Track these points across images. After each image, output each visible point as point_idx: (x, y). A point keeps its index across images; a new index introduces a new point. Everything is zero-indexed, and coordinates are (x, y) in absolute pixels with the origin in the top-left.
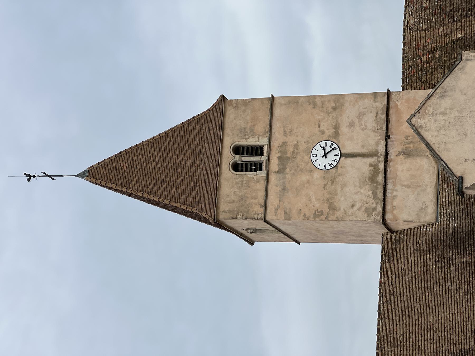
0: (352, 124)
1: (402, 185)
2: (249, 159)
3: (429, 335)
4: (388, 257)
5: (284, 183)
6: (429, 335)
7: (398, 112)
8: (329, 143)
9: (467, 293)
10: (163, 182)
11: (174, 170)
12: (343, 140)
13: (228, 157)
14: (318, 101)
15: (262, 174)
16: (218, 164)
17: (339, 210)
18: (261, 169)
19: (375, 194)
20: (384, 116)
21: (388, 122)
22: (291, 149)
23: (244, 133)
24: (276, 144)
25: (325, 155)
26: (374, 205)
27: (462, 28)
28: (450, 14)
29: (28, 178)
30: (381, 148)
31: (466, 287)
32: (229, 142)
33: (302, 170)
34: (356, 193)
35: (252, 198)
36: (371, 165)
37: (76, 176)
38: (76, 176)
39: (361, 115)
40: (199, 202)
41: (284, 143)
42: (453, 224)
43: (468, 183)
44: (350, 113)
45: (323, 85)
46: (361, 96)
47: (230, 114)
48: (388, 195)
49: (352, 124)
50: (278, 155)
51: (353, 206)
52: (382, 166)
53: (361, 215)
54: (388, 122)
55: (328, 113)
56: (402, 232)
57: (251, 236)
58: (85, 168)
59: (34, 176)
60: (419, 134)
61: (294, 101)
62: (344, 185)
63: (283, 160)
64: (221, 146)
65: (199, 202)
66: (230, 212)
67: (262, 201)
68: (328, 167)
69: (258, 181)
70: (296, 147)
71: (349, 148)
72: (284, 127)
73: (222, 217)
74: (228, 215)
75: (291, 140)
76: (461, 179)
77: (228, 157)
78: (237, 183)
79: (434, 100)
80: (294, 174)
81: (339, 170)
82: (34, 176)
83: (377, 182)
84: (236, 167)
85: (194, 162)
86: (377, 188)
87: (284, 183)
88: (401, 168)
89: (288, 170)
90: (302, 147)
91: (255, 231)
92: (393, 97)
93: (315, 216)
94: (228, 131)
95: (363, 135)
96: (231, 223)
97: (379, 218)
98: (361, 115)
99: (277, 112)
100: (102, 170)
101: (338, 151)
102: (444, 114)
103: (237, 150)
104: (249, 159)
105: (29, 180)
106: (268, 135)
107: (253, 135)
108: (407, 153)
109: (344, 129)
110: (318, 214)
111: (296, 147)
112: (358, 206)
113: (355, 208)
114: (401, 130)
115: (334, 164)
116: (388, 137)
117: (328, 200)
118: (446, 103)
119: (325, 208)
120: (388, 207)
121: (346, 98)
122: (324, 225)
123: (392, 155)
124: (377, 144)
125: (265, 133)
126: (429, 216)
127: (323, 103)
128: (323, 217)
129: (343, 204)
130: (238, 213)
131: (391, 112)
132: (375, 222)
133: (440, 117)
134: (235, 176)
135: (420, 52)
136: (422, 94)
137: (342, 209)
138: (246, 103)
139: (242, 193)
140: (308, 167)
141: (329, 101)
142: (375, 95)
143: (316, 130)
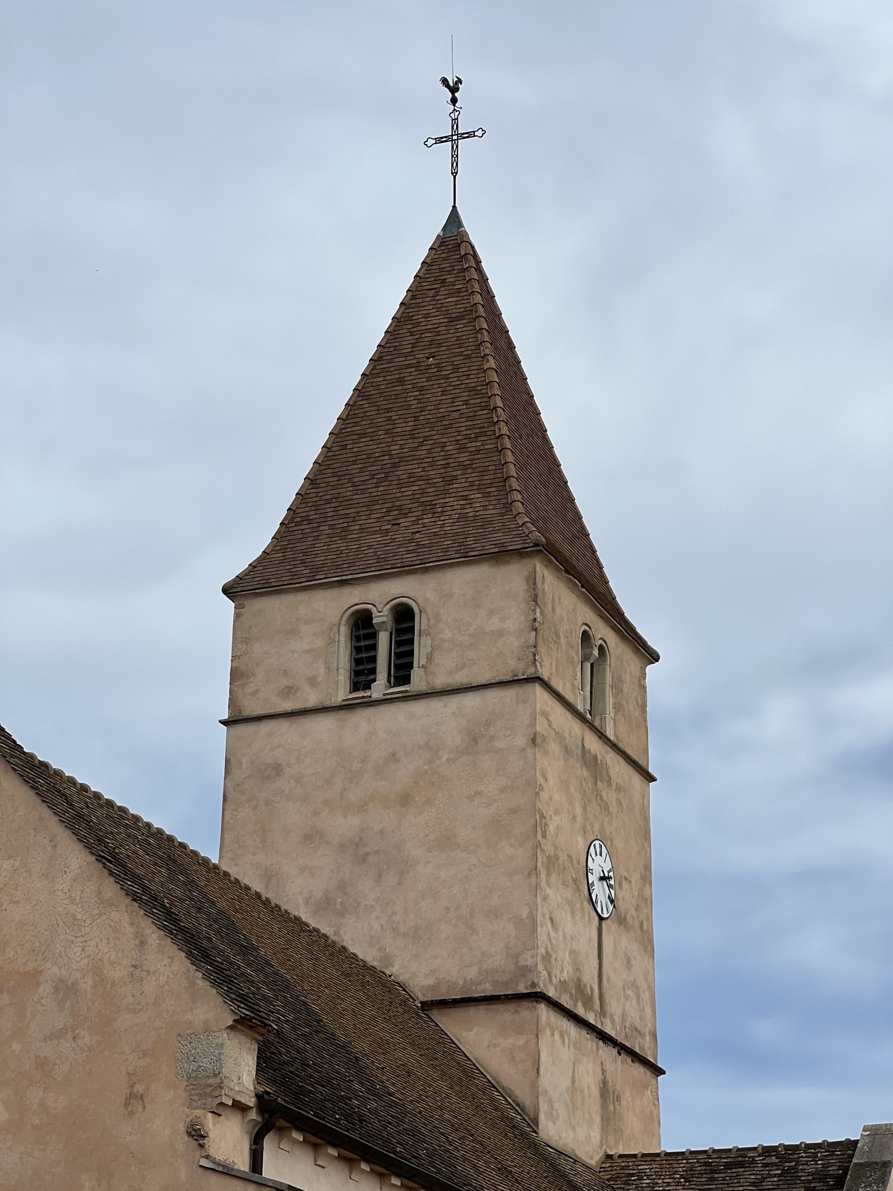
22: (604, 794)
29: (451, 84)
30: (608, 1029)
34: (564, 934)
37: (454, 207)
38: (454, 207)
48: (566, 1025)
49: (629, 965)
59: (454, 101)
70: (607, 809)
81: (588, 907)
82: (454, 101)
105: (445, 81)
116: (622, 1049)
119: (549, 849)
123: (607, 1052)
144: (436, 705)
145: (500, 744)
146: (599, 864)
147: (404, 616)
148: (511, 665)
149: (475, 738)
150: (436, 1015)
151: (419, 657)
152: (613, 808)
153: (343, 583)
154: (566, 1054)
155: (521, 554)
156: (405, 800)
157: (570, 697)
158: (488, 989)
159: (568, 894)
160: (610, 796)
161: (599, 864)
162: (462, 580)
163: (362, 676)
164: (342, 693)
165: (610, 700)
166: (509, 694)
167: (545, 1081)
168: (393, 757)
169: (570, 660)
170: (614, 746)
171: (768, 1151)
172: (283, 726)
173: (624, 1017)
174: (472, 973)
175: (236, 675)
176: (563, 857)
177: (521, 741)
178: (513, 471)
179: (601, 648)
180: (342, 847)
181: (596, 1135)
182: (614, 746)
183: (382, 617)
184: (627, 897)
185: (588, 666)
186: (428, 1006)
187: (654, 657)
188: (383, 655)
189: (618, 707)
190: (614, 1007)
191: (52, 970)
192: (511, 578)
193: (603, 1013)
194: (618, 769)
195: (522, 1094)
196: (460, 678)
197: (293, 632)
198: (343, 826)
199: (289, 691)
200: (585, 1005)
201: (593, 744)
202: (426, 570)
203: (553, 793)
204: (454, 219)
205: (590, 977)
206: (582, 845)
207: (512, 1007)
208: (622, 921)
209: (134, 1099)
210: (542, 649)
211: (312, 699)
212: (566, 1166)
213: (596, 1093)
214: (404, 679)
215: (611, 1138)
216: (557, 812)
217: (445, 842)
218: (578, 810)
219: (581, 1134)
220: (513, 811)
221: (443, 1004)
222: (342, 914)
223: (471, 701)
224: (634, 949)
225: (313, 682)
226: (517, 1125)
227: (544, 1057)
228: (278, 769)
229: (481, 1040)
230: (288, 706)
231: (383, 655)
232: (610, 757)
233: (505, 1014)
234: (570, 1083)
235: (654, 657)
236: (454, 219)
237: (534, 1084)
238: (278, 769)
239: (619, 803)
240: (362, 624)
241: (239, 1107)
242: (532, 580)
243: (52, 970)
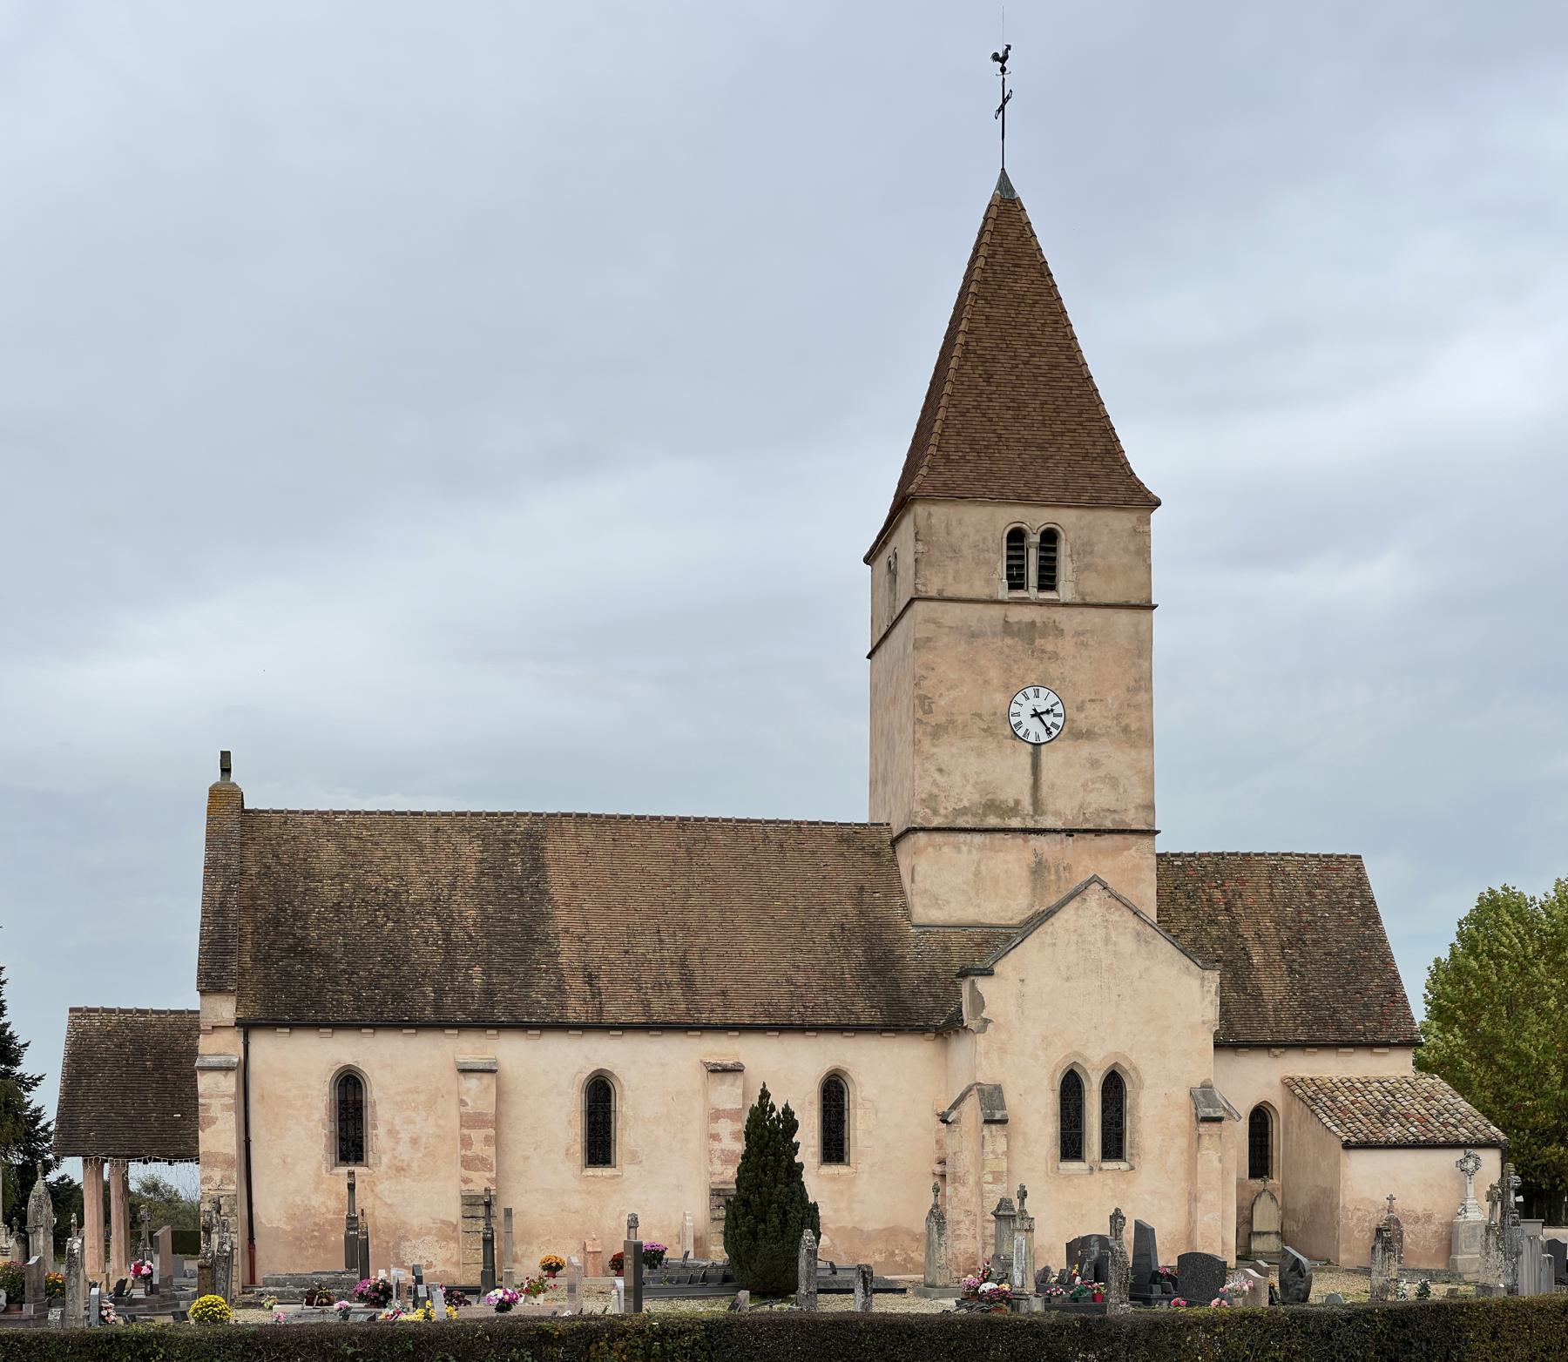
0: (1095, 764)
1: (979, 863)
2: (1032, 562)
3: (713, 914)
4: (848, 836)
5: (984, 634)
6: (713, 914)
7: (1117, 851)
8: (1059, 721)
9: (789, 981)
10: (988, 378)
11: (1013, 401)
13: (1035, 519)
14: (1141, 697)
15: (1003, 592)
16: (1022, 500)
17: (934, 745)
18: (1012, 587)
20: (1109, 825)
21: (1098, 832)
22: (1050, 647)
23: (1083, 550)
24: (1060, 615)
25: (1036, 714)
26: (943, 812)
27: (1269, 964)
28: (1297, 941)
30: (1048, 822)
31: (800, 979)
32: (1066, 520)
33: (1008, 669)
34: (964, 776)
35: (956, 571)
36: (1017, 802)
39: (1113, 781)
40: (948, 460)
42: (910, 953)
43: (983, 984)
44: (1117, 759)
45: (1170, 711)
46: (1149, 781)
47: (1120, 521)
48: (962, 837)
49: (1095, 764)
50: (1038, 621)
51: (940, 770)
52: (1015, 823)
53: (924, 787)
54: (1098, 832)
55: (1117, 717)
56: (894, 861)
57: (882, 560)
58: (1020, 192)
59: (1003, 70)
60: (1071, 897)
61: (1143, 647)
62: (980, 753)
63: (1029, 632)
64: (1059, 504)
65: (948, 460)
66: (930, 526)
67: (948, 593)
68: (1014, 720)
69: (988, 582)
70: (1054, 656)
71: (1048, 758)
72: (1093, 632)
73: (919, 510)
74: (922, 523)
75: (1066, 646)
77: (1035, 519)
78: (985, 539)
79: (1133, 922)
80: (1001, 653)
82: (1003, 70)
83: (985, 815)
84: (1016, 537)
85: (1027, 445)
86: (974, 815)
87: (984, 634)
88: (1012, 858)
89: (1008, 641)
90: (1054, 669)
91: (892, 571)
92: (1146, 841)
93: (923, 699)
94: (1088, 516)
95: (1072, 789)
96: (906, 526)
97: (919, 822)
98: (1113, 781)
99: (1123, 618)
100: (1013, 233)
101: (1044, 738)
102: (1107, 941)
103: (1050, 538)
104: (1032, 562)
105: (995, 57)
106: (1078, 600)
107: (1077, 570)
108: (1038, 869)
109: (1086, 749)
110: (925, 703)
111: (1054, 656)
112: (941, 780)
113: (937, 775)
114: (1084, 859)
115: (1020, 733)
116: (1070, 833)
117: (952, 722)
118: (1127, 944)
120: (938, 838)
121: (1145, 752)
122: (906, 711)
123: (1036, 842)
124: (1057, 814)
125: (1083, 595)
126: (924, 912)
127: (1137, 707)
128: (920, 714)
129: (945, 751)
130: (927, 543)
131: (1118, 838)
132: (912, 814)
133: (1101, 932)
134: (998, 535)
135: (1231, 885)
136: (1147, 895)
137: (934, 750)
138: (1144, 553)
139: (967, 552)
140: (1014, 681)
141: (1141, 719)
142: (1150, 807)
143: (1085, 695)
157: (980, 591)
187: (1158, 504)
200: (1001, 817)
227: (918, 869)
234: (971, 876)
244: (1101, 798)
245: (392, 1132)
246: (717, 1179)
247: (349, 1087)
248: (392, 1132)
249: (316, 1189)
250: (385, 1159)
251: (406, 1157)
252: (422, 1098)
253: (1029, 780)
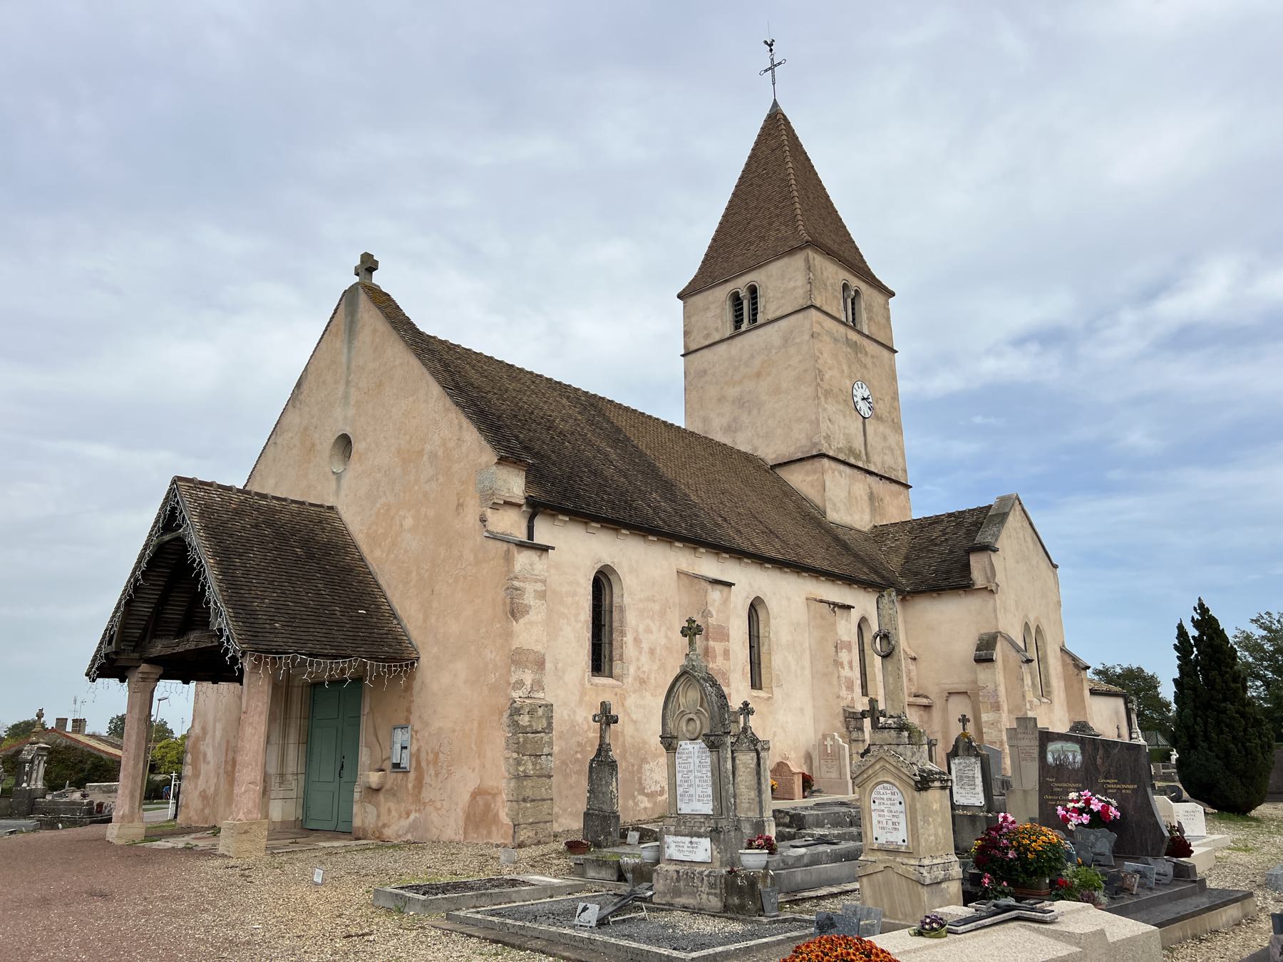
12: (873, 421)
14: (896, 404)
19: (840, 450)
23: (869, 308)
30: (872, 469)
32: (863, 287)
39: (892, 450)
41: (866, 354)
44: (892, 439)
48: (842, 467)
49: (885, 438)
52: (860, 465)
63: (854, 346)
67: (824, 308)
70: (865, 366)
71: (870, 429)
76: (995, 550)
81: (854, 413)
97: (824, 451)
98: (892, 450)
99: (885, 353)
109: (881, 428)
116: (882, 477)
119: (826, 386)
123: (870, 479)
129: (831, 408)
144: (769, 328)
145: (798, 340)
146: (861, 392)
147: (753, 290)
148: (802, 302)
149: (786, 340)
150: (777, 471)
151: (760, 308)
152: (870, 365)
153: (726, 281)
154: (844, 481)
155: (800, 248)
156: (758, 375)
157: (837, 315)
158: (800, 455)
159: (841, 407)
160: (868, 361)
161: (861, 392)
162: (775, 268)
163: (738, 322)
164: (729, 330)
165: (865, 316)
166: (800, 316)
167: (828, 494)
168: (752, 356)
169: (835, 297)
170: (867, 337)
171: (950, 515)
172: (705, 352)
173: (883, 463)
174: (792, 449)
175: (686, 333)
176: (835, 390)
177: (807, 337)
178: (799, 212)
179: (856, 291)
180: (734, 402)
181: (867, 517)
182: (867, 337)
183: (743, 293)
184: (882, 408)
185: (849, 301)
186: (773, 467)
187: (893, 294)
188: (745, 312)
189: (870, 319)
190: (876, 458)
191: (428, 447)
192: (797, 261)
193: (868, 461)
194: (872, 348)
195: (818, 501)
196: (778, 314)
197: (707, 309)
198: (732, 392)
199: (708, 335)
201: (853, 336)
202: (760, 267)
203: (826, 357)
204: (775, 104)
205: (858, 444)
206: (848, 383)
207: (810, 462)
208: (879, 418)
209: (460, 506)
210: (815, 292)
211: (717, 337)
212: (840, 531)
213: (866, 498)
214: (755, 321)
215: (878, 518)
216: (830, 369)
217: (776, 391)
218: (845, 368)
219: (857, 517)
220: (806, 371)
221: (780, 465)
222: (735, 432)
223: (783, 323)
224: (888, 431)
225: (717, 330)
226: (812, 517)
227: (828, 484)
228: (705, 372)
229: (798, 479)
230: (707, 343)
231: (745, 312)
232: (866, 342)
233: (808, 466)
235: (893, 294)
236: (775, 104)
237: (823, 496)
238: (705, 372)
239: (874, 364)
240: (736, 299)
241: (519, 506)
242: (807, 260)
243: (428, 447)
244: (889, 460)
245: (637, 641)
246: (844, 703)
247: (602, 583)
248: (637, 641)
249: (581, 701)
250: (632, 670)
251: (646, 668)
252: (657, 607)
253: (862, 439)
